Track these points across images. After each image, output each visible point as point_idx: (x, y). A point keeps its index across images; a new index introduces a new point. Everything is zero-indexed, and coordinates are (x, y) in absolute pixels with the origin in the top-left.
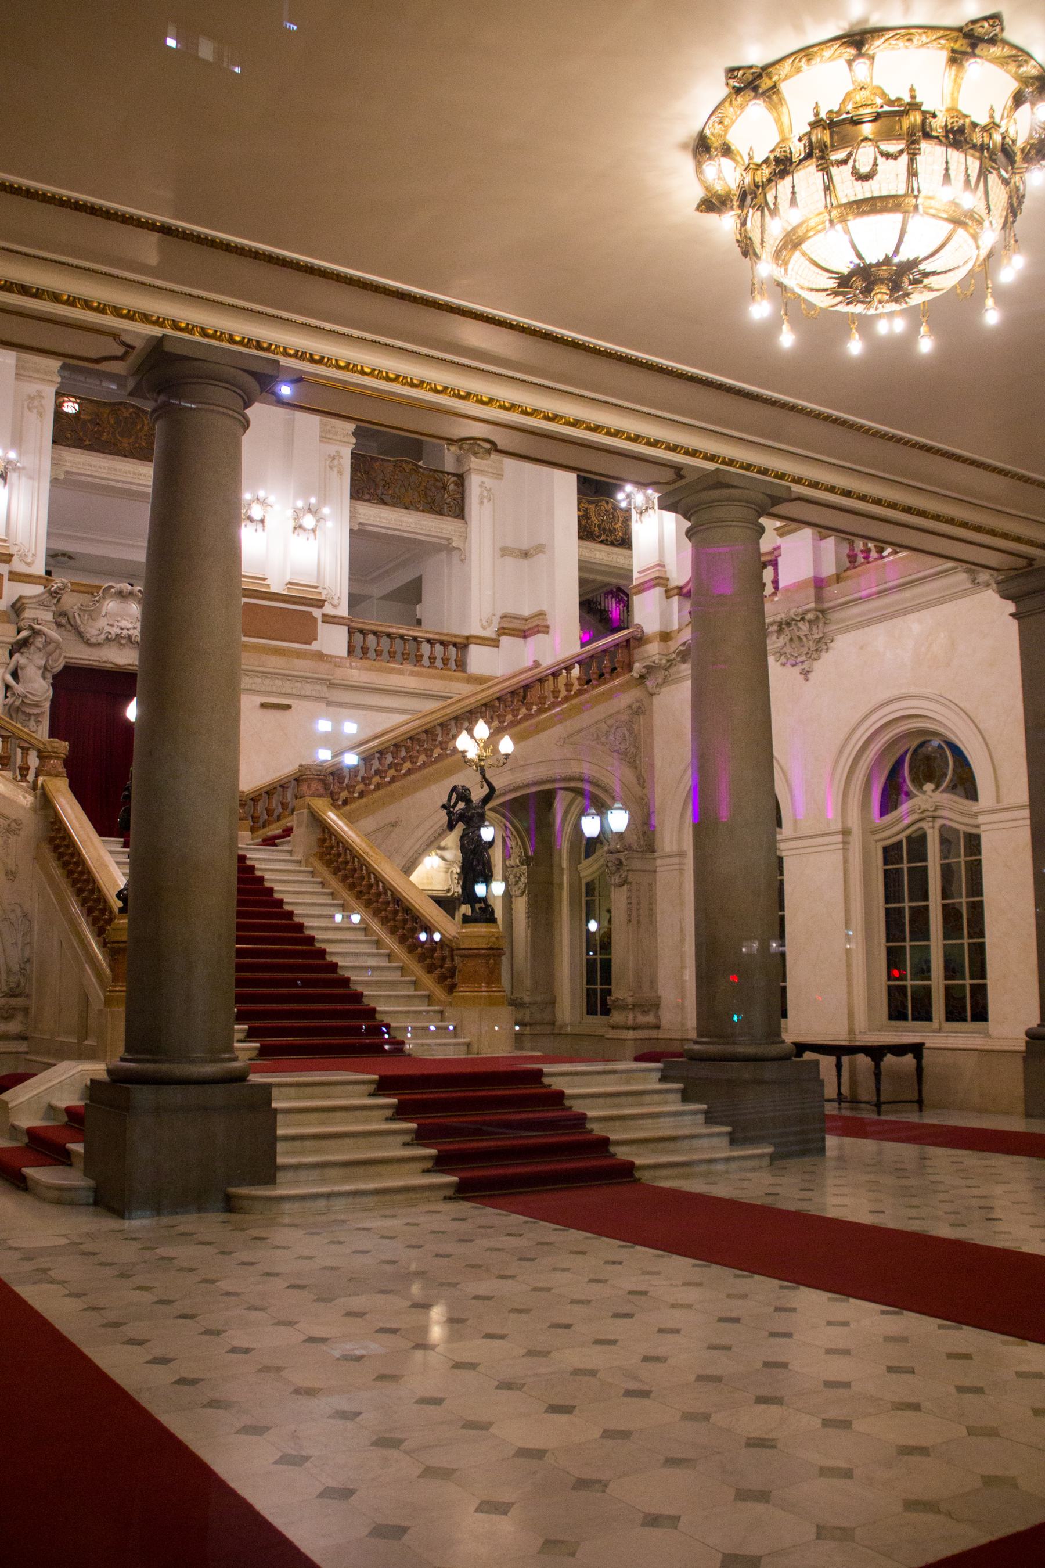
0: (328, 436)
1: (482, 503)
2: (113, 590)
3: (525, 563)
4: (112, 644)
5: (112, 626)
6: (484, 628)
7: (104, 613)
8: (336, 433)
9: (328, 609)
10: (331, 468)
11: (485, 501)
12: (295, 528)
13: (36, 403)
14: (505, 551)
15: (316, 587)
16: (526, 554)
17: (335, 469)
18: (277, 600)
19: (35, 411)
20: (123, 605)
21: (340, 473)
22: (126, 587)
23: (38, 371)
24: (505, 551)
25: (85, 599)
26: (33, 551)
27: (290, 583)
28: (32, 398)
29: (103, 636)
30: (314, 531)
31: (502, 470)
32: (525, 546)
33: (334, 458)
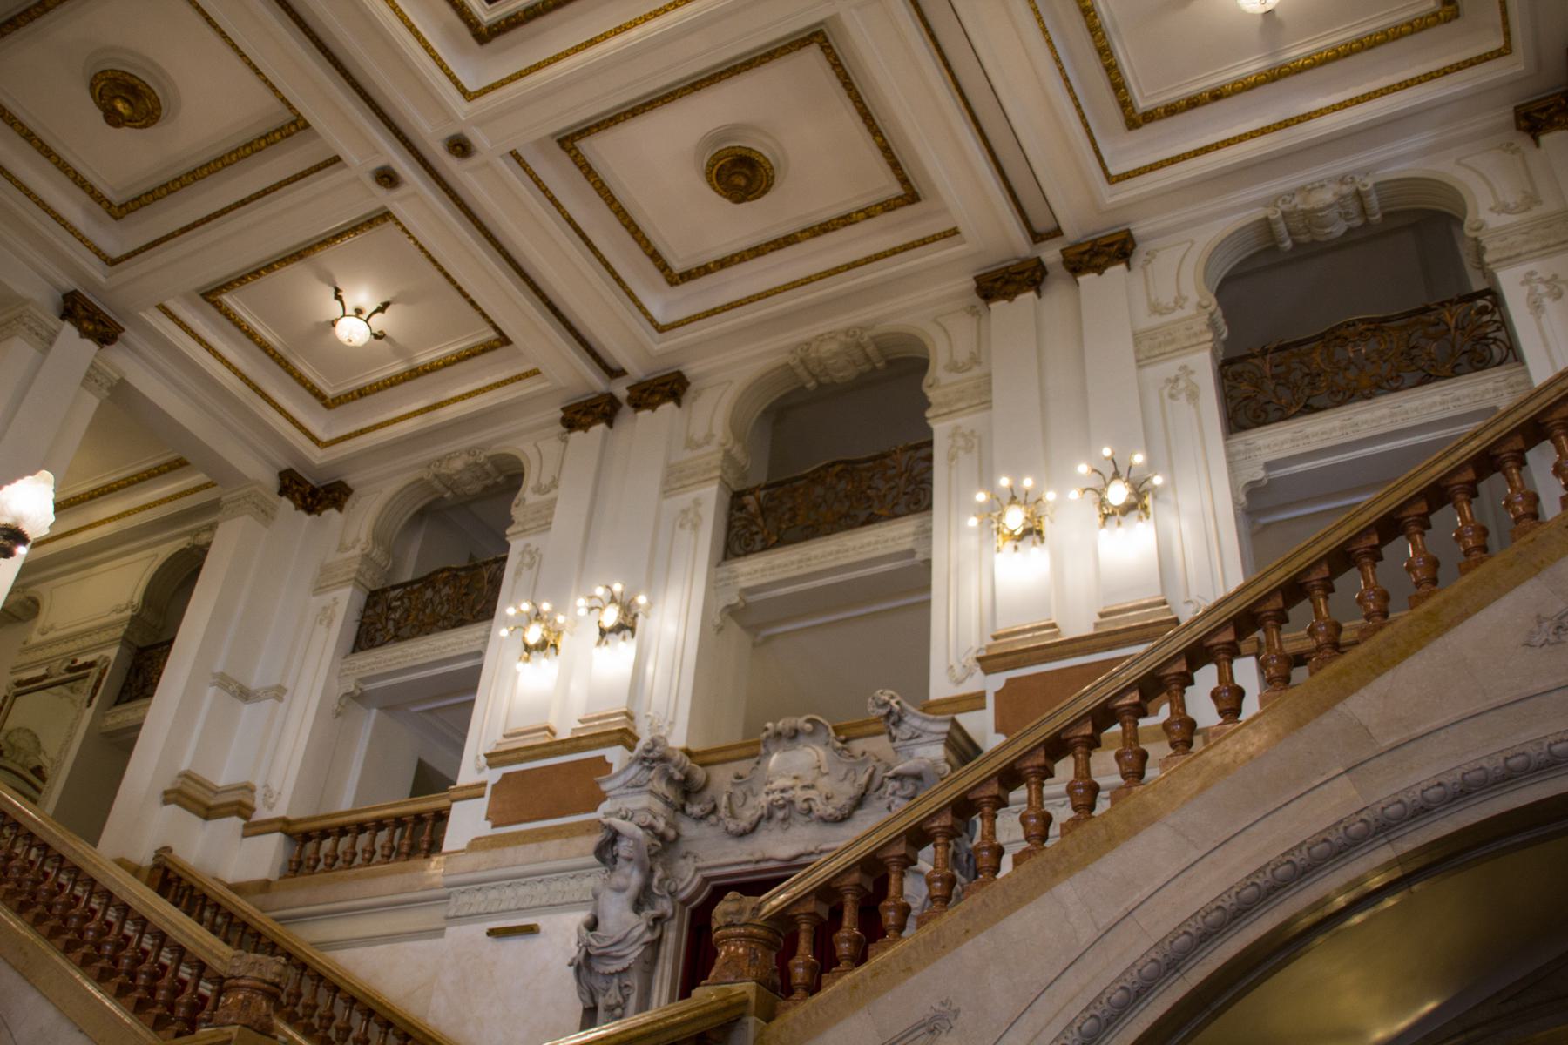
4: (772, 824)
8: (1173, 341)
10: (1172, 396)
11: (1547, 301)
13: (691, 515)
15: (1165, 603)
18: (1074, 654)
20: (788, 754)
21: (1193, 396)
22: (783, 724)
25: (743, 767)
26: (670, 718)
28: (685, 512)
33: (1177, 379)
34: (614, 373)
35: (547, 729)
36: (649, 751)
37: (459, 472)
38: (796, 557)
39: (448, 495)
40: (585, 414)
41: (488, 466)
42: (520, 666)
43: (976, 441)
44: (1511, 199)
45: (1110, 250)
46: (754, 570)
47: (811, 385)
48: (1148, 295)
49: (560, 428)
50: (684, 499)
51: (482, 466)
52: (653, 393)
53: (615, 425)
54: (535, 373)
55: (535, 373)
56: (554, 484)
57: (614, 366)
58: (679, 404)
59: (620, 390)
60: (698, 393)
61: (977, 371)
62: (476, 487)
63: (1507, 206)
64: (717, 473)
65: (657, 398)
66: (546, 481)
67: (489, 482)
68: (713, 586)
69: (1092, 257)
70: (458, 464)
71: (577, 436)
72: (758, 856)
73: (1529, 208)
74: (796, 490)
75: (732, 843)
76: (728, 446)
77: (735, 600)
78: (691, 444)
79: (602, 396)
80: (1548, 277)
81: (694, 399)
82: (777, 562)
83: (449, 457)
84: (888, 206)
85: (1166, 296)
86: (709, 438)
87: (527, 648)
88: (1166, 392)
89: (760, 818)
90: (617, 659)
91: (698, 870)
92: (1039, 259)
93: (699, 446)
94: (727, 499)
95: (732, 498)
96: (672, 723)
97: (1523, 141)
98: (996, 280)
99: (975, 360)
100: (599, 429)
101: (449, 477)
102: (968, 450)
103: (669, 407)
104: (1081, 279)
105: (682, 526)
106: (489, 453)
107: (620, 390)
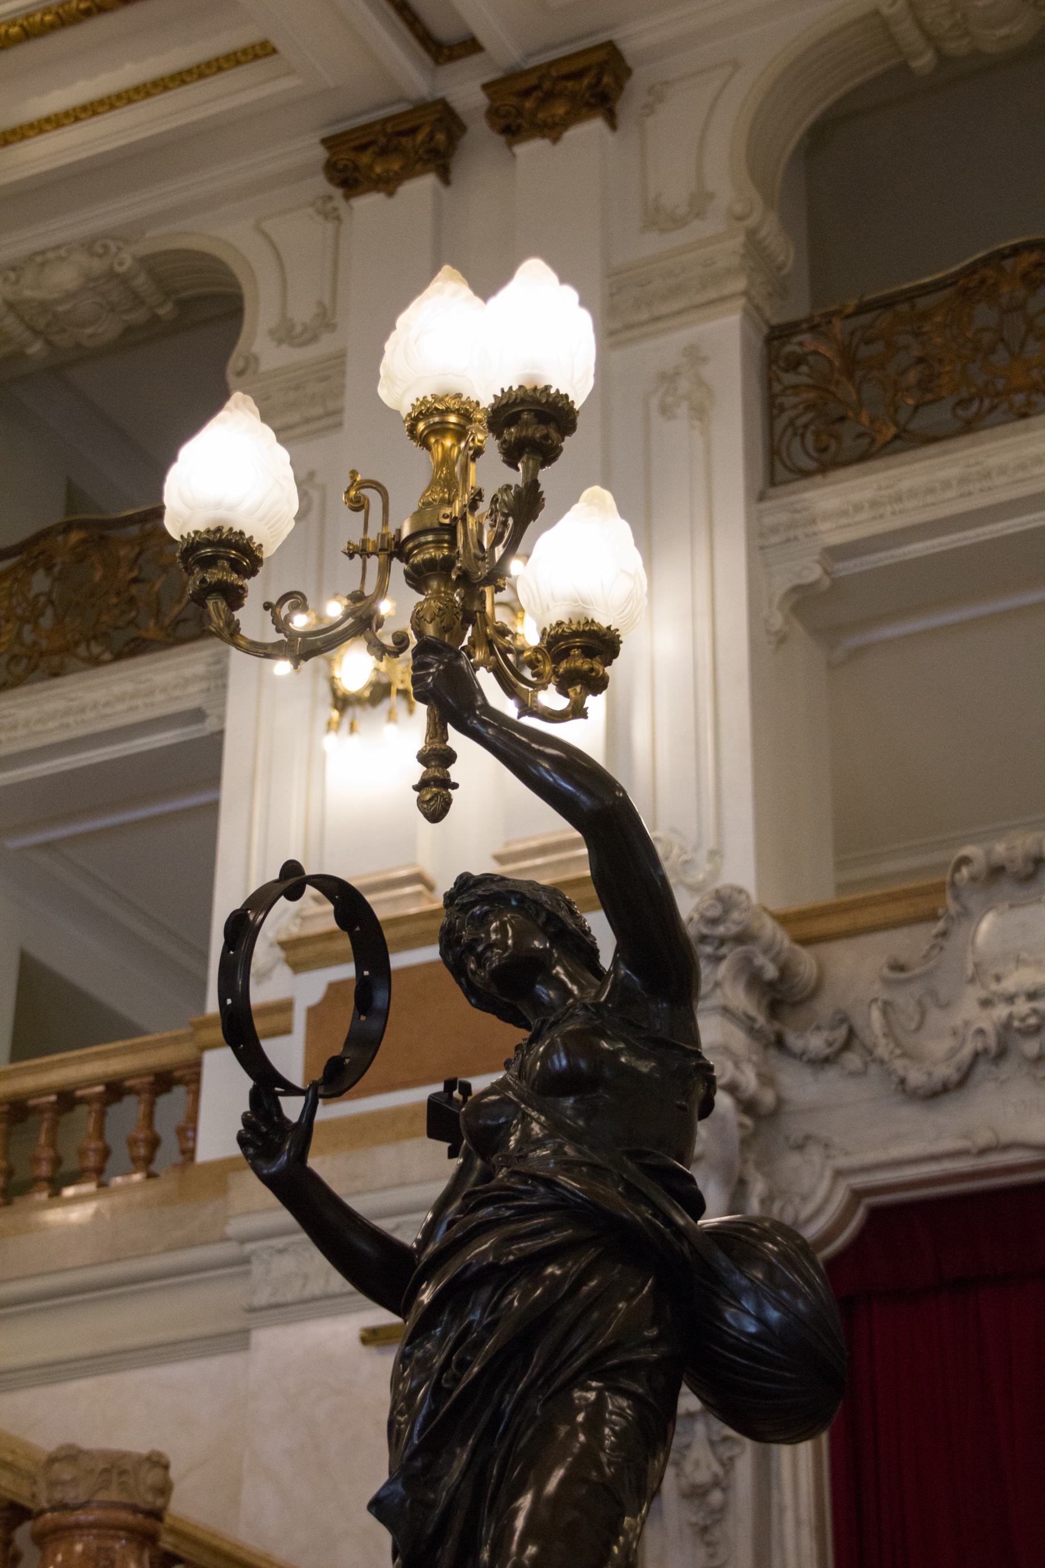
2: (965, 871)
4: (1008, 1068)
5: (986, 1003)
7: (970, 970)
13: (684, 385)
19: (683, 410)
20: (1025, 915)
25: (909, 942)
26: (710, 844)
28: (668, 378)
29: (967, 1051)
34: (445, 50)
35: (418, 878)
36: (714, 922)
37: (70, 296)
38: (952, 472)
39: (36, 348)
40: (384, 152)
41: (141, 281)
42: (330, 742)
46: (850, 504)
47: (924, 61)
49: (321, 184)
50: (665, 347)
51: (124, 280)
52: (549, 97)
53: (455, 174)
54: (261, 51)
55: (261, 51)
56: (326, 320)
57: (443, 30)
59: (465, 89)
60: (657, 94)
62: (108, 329)
64: (740, 284)
65: (560, 109)
66: (302, 313)
67: (138, 316)
68: (761, 547)
70: (66, 277)
71: (368, 203)
72: (984, 1138)
74: (925, 316)
75: (910, 1114)
76: (751, 222)
77: (815, 573)
78: (657, 218)
79: (422, 107)
81: (649, 109)
82: (905, 485)
83: (40, 260)
86: (700, 202)
87: (343, 702)
89: (976, 1056)
91: (839, 1174)
93: (678, 222)
94: (758, 343)
95: (769, 340)
96: (715, 854)
100: (422, 187)
101: (44, 306)
103: (590, 131)
106: (142, 249)
107: (465, 89)
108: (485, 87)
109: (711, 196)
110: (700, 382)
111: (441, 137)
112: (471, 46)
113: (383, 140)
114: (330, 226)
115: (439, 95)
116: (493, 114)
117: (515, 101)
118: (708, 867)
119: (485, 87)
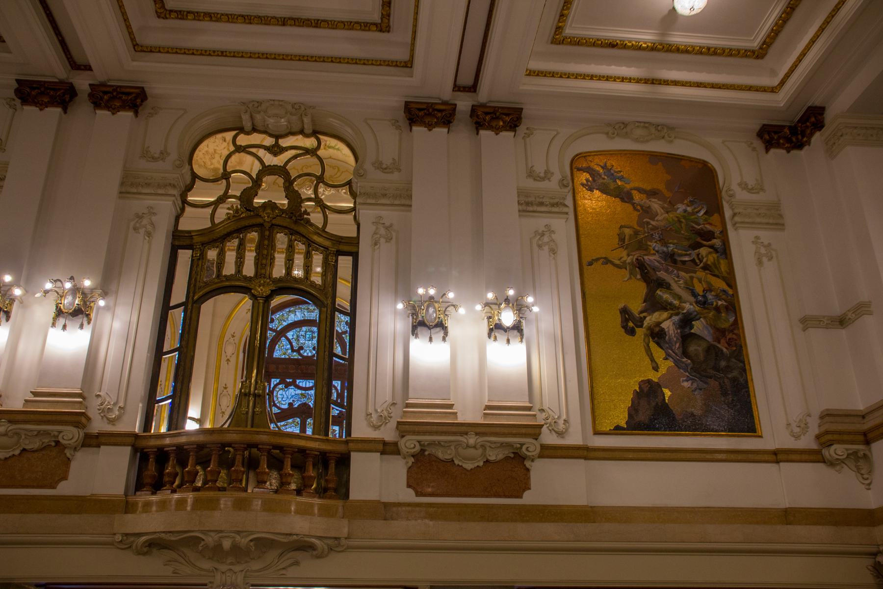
0: (531, 209)
1: (760, 263)
3: (843, 333)
6: (797, 437)
8: (541, 204)
9: (548, 438)
10: (540, 246)
11: (765, 259)
12: (491, 330)
13: (145, 221)
14: (807, 322)
15: (529, 409)
16: (842, 322)
17: (546, 248)
19: (142, 231)
23: (148, 185)
24: (807, 322)
27: (488, 407)
28: (140, 217)
30: (517, 328)
31: (781, 216)
32: (837, 308)
33: (543, 235)
34: (78, 66)
43: (394, 234)
44: (751, 183)
45: (504, 118)
48: (527, 165)
50: (138, 205)
58: (136, 113)
61: (396, 176)
63: (746, 184)
69: (492, 118)
73: (758, 193)
79: (61, 82)
80: (766, 243)
84: (365, 26)
85: (540, 169)
88: (535, 241)
90: (69, 343)
92: (456, 105)
93: (154, 159)
97: (759, 145)
98: (420, 110)
99: (395, 167)
102: (389, 240)
104: (482, 132)
105: (135, 229)
107: (82, 82)
108: (90, 85)
109: (168, 154)
110: (152, 224)
111: (67, 97)
112: (88, 68)
113: (42, 89)
114: (11, 111)
115: (71, 81)
116: (91, 96)
117: (101, 94)
118: (117, 413)
119: (90, 85)
